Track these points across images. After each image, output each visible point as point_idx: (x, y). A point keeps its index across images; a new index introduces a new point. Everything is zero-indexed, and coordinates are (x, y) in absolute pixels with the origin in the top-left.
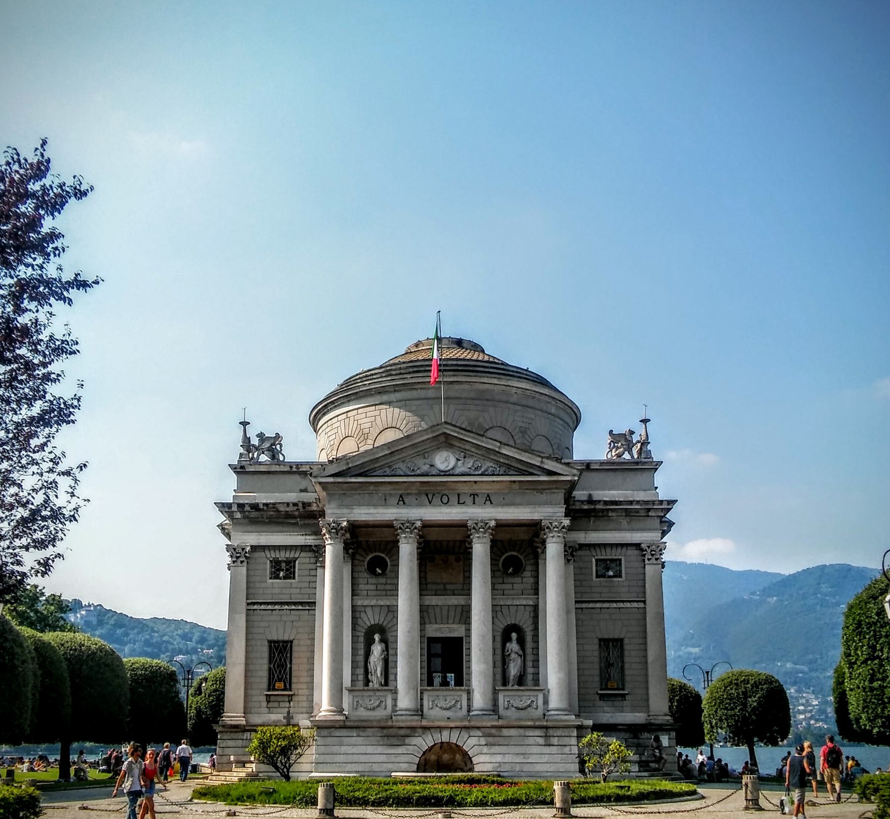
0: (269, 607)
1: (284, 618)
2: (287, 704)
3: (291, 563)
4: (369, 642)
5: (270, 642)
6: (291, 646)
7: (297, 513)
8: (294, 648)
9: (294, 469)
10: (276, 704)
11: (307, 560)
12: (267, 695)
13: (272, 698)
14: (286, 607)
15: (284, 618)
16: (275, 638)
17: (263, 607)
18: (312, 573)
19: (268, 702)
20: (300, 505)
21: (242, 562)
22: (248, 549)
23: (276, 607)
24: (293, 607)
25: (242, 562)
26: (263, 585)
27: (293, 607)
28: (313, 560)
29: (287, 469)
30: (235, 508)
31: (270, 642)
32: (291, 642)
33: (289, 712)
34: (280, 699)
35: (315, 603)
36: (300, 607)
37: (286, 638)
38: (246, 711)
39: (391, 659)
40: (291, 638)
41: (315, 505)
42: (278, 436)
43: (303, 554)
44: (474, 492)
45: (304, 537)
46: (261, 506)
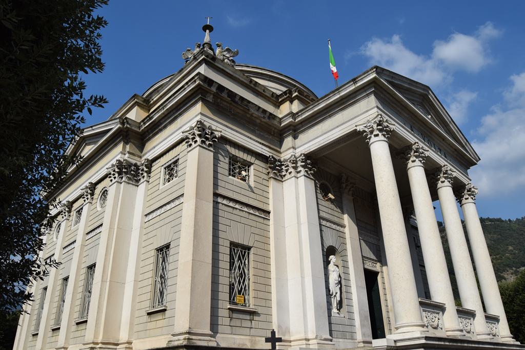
0: (231, 204)
1: (243, 220)
2: (248, 324)
3: (246, 165)
4: (327, 263)
5: (232, 243)
6: (249, 253)
7: (258, 121)
8: (251, 256)
9: (252, 86)
10: (238, 323)
11: (261, 169)
12: (229, 309)
13: (235, 315)
14: (246, 209)
15: (243, 220)
16: (236, 241)
17: (225, 202)
18: (265, 182)
19: (231, 318)
20: (268, 114)
21: (210, 145)
22: (218, 134)
23: (237, 206)
24: (251, 211)
25: (210, 145)
26: (225, 178)
27: (251, 211)
28: (265, 171)
29: (248, 83)
30: (214, 89)
31: (232, 243)
32: (249, 248)
33: (273, 333)
34: (241, 316)
35: (269, 213)
36: (257, 214)
37: (246, 243)
38: (214, 326)
39: (343, 282)
40: (250, 245)
41: (278, 120)
42: (236, 54)
43: (257, 162)
44: (441, 148)
45: (260, 146)
46: (237, 99)
